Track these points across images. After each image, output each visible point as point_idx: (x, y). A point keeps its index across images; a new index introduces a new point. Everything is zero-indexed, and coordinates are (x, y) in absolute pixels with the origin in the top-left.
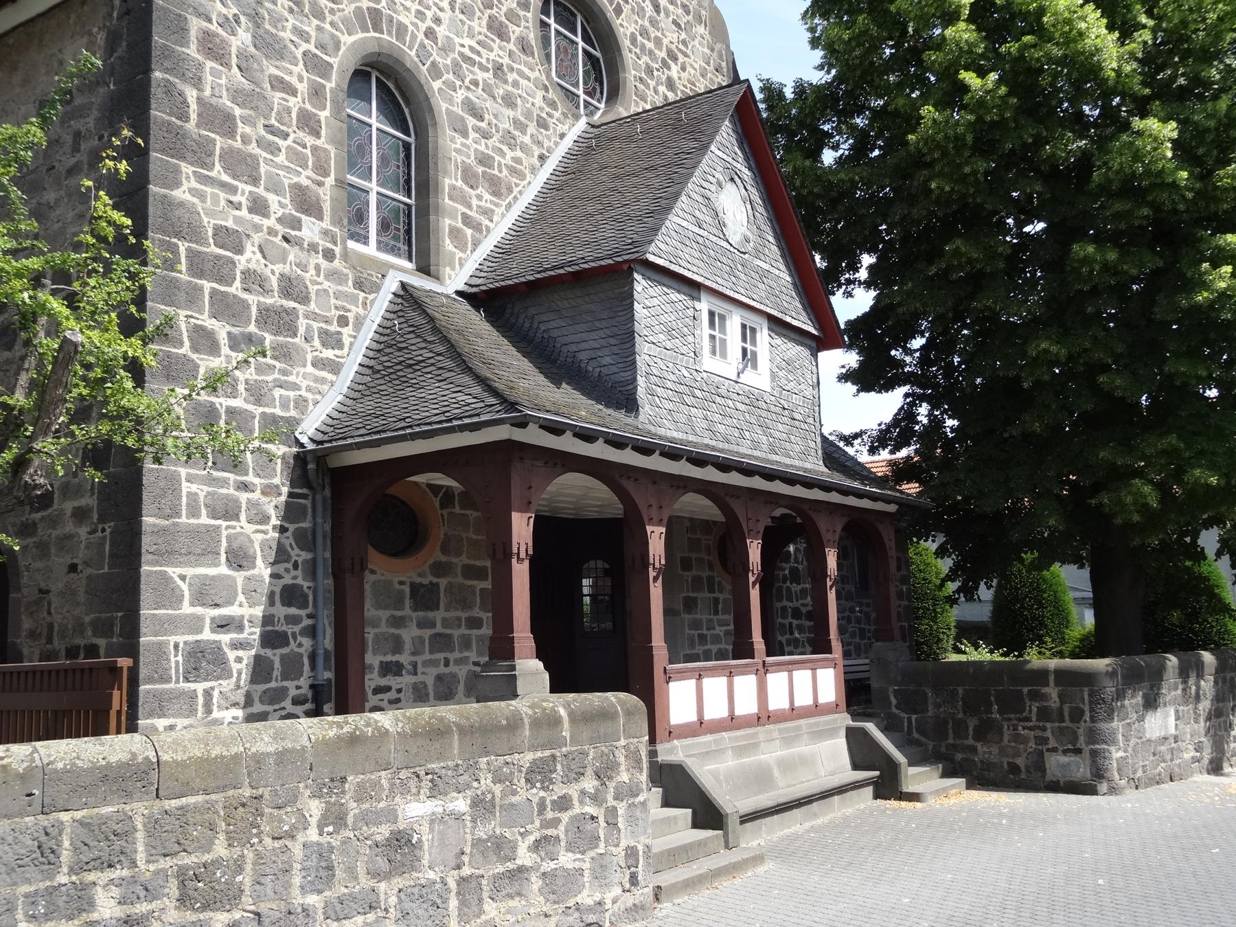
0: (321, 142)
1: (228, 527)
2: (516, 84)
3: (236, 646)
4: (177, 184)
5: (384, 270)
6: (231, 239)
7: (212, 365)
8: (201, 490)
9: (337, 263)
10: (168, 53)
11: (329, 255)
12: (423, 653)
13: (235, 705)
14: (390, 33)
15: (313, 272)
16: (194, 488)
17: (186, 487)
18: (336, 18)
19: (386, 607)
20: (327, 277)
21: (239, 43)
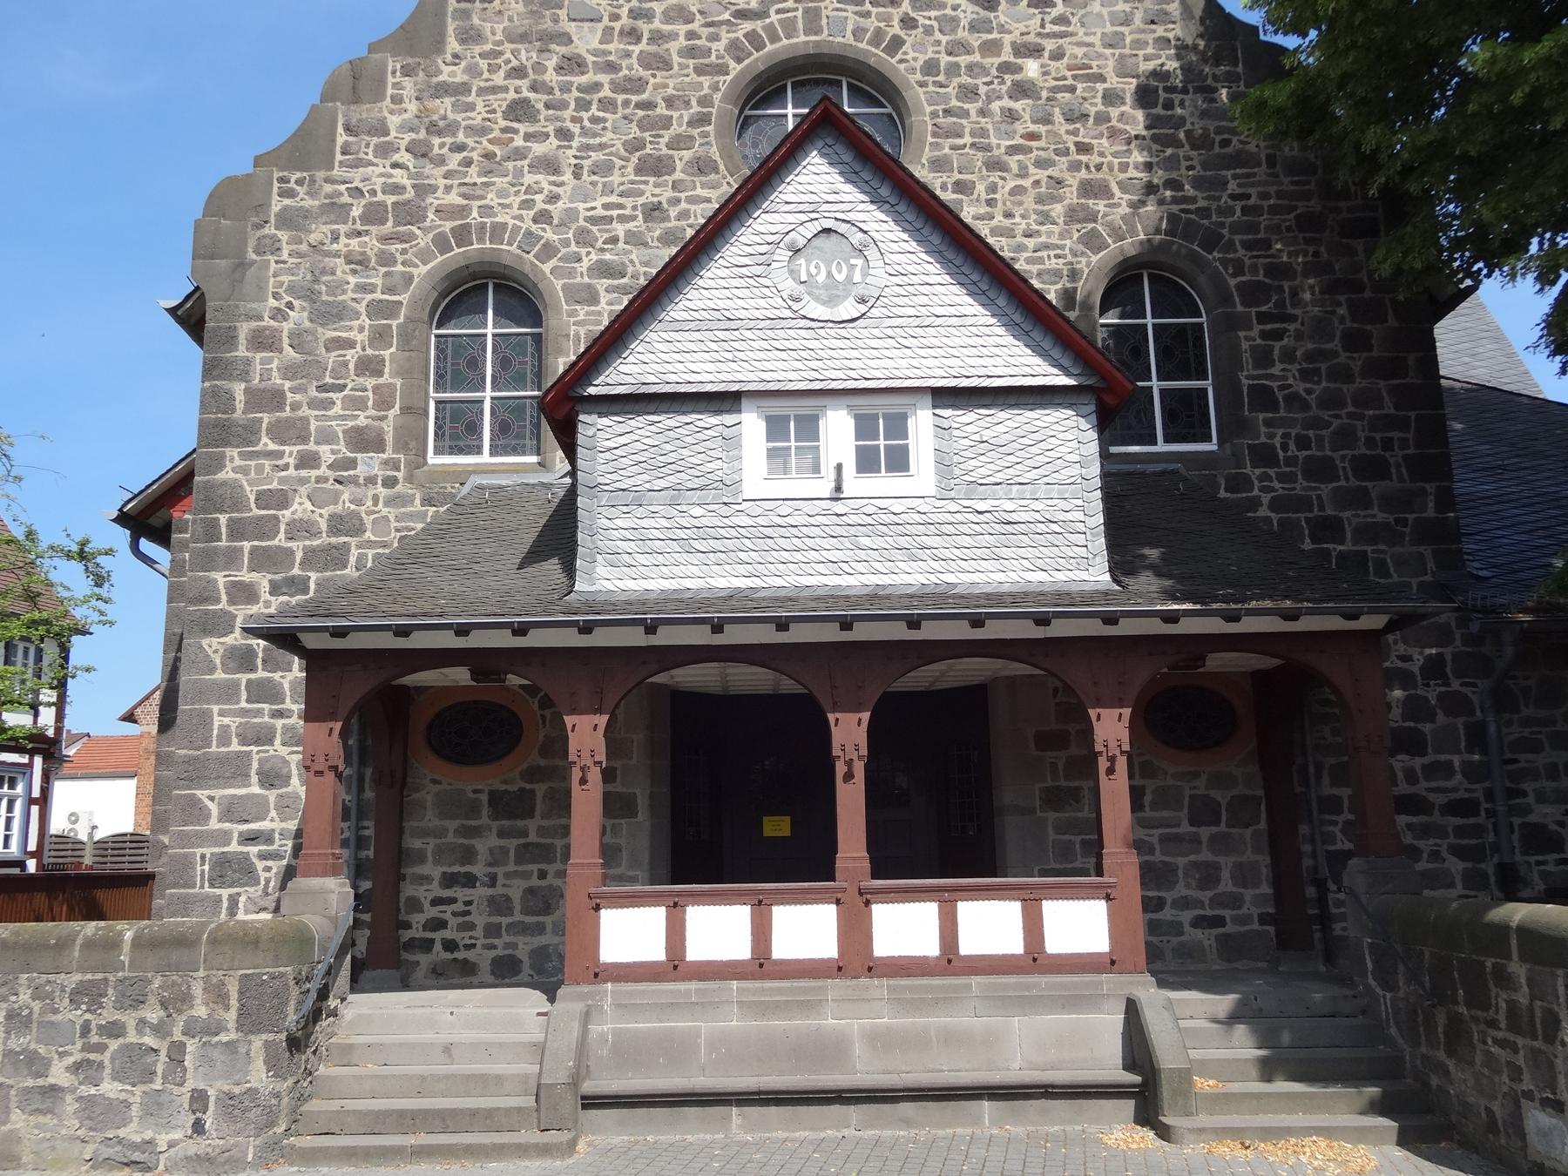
0: (386, 378)
3: (263, 856)
4: (221, 467)
7: (251, 612)
8: (232, 722)
9: (399, 488)
12: (505, 864)
13: (264, 909)
14: (481, 240)
15: (369, 503)
16: (226, 720)
20: (386, 504)
21: (292, 325)
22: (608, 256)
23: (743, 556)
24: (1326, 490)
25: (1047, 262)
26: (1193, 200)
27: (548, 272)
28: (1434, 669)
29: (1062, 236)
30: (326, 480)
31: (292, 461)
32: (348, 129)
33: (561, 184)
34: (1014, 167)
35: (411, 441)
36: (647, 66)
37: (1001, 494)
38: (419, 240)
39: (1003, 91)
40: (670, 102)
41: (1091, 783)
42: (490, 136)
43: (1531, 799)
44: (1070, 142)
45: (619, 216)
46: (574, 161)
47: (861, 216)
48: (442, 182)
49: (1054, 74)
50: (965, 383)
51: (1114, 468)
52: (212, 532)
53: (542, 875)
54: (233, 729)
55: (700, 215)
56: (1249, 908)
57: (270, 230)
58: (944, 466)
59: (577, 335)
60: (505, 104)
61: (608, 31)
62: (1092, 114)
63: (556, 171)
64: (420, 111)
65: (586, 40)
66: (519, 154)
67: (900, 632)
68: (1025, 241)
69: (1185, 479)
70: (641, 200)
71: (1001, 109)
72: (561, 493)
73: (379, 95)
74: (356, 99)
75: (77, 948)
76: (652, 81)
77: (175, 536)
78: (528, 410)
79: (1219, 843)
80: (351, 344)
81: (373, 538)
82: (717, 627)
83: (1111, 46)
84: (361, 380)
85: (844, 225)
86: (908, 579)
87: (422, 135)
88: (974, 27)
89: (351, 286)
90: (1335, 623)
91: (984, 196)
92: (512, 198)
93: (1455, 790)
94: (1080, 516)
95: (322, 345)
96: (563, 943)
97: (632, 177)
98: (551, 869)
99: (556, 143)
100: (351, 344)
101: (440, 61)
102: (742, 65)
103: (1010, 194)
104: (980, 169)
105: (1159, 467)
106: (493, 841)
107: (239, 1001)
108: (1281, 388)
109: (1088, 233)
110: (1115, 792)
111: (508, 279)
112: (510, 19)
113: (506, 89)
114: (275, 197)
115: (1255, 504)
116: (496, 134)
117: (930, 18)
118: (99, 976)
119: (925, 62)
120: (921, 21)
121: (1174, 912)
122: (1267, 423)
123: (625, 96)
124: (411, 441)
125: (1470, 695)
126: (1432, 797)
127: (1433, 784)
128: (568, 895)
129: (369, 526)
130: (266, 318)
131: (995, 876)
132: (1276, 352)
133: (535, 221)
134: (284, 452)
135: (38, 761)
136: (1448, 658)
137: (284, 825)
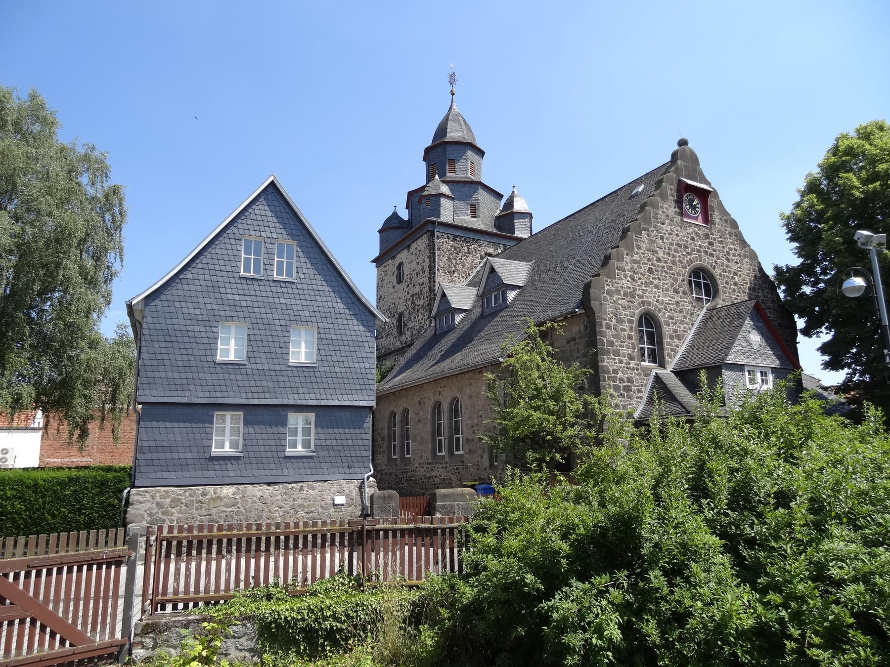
0: (633, 341)
2: (683, 305)
5: (651, 369)
6: (616, 371)
10: (600, 332)
11: (637, 369)
66: (651, 283)
80: (625, 330)
100: (625, 330)
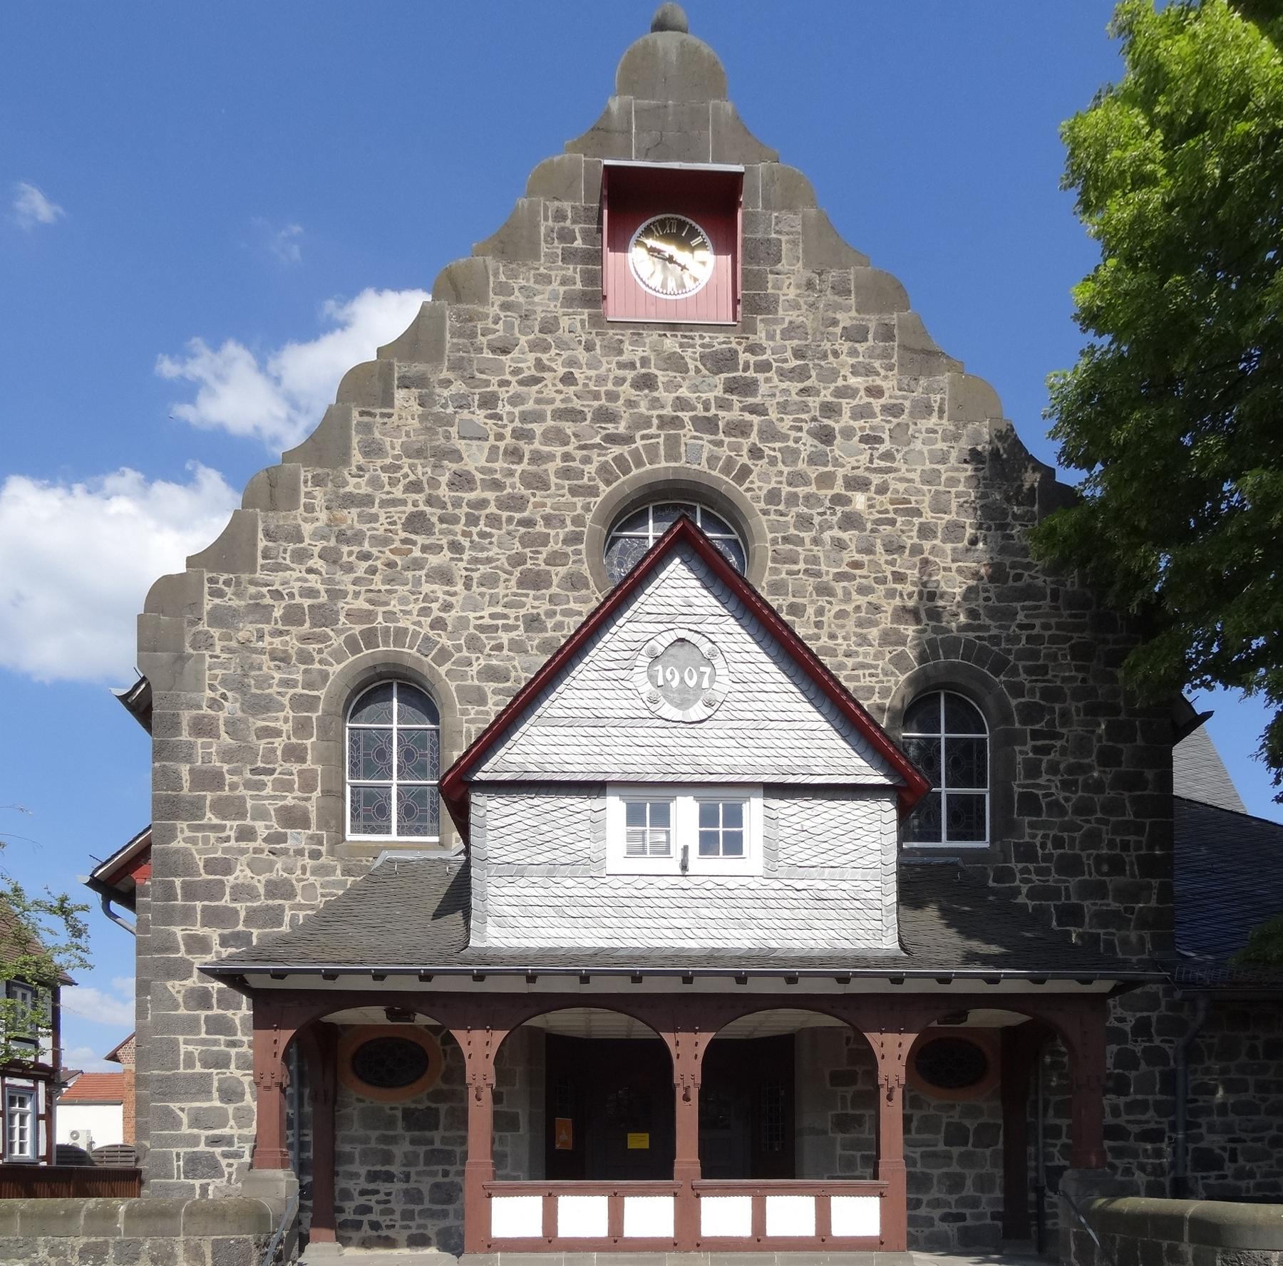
1: (218, 1074)
3: (225, 1155)
4: (174, 837)
8: (196, 1050)
9: (323, 860)
14: (386, 643)
15: (299, 872)
16: (190, 1048)
17: (183, 1048)
18: (324, 655)
19: (375, 1128)
20: (313, 874)
21: (227, 714)
22: (494, 662)
23: (606, 921)
24: (1073, 882)
25: (862, 680)
26: (987, 628)
27: (443, 674)
28: (1142, 1028)
29: (876, 657)
30: (262, 851)
31: (232, 834)
32: (267, 535)
33: (453, 594)
34: (840, 592)
35: (332, 819)
36: (528, 485)
37: (815, 875)
38: (333, 641)
39: (834, 522)
40: (548, 520)
41: (873, 1112)
42: (392, 547)
43: (1203, 1130)
44: (888, 570)
45: (503, 625)
46: (465, 573)
47: (711, 628)
48: (351, 588)
49: (878, 508)
50: (791, 779)
51: (906, 860)
52: (169, 893)
53: (446, 1174)
54: (196, 1055)
55: (572, 624)
56: (986, 1209)
57: (203, 627)
58: (771, 851)
59: (468, 731)
60: (404, 517)
61: (494, 449)
62: (908, 546)
63: (450, 582)
64: (330, 519)
65: (474, 458)
66: (417, 564)
67: (730, 987)
68: (845, 660)
69: (962, 870)
70: (522, 612)
71: (832, 538)
72: (457, 868)
73: (293, 504)
74: (273, 506)
75: (82, 1218)
76: (532, 499)
77: (139, 900)
78: (429, 796)
79: (966, 1160)
80: (277, 733)
81: (303, 902)
82: (585, 979)
83: (929, 483)
84: (287, 765)
85: (696, 635)
86: (737, 944)
87: (333, 543)
88: (812, 460)
89: (276, 681)
90: (1072, 987)
91: (813, 619)
92: (411, 606)
93: (1148, 1122)
94: (877, 895)
95: (253, 733)
96: (463, 1226)
97: (515, 590)
98: (452, 1169)
99: (450, 555)
100: (277, 733)
101: (346, 473)
102: (611, 488)
103: (834, 618)
104: (811, 593)
105: (941, 860)
106: (406, 1147)
107: (213, 1258)
108: (1045, 796)
109: (897, 655)
110: (892, 1113)
111: (410, 680)
112: (408, 435)
113: (403, 502)
114: (207, 597)
115: (1016, 892)
116: (397, 544)
117: (774, 450)
118: (101, 1239)
119: (769, 491)
120: (767, 452)
121: (928, 1210)
122: (1032, 825)
123: (509, 513)
124: (332, 819)
125: (1167, 1049)
126: (1130, 1127)
127: (1131, 1118)
128: (466, 1188)
129: (299, 891)
130: (205, 708)
131: (793, 1177)
132: (1044, 765)
133: (432, 627)
134: (225, 825)
135: (42, 1086)
136: (1154, 1020)
137: (241, 1131)
